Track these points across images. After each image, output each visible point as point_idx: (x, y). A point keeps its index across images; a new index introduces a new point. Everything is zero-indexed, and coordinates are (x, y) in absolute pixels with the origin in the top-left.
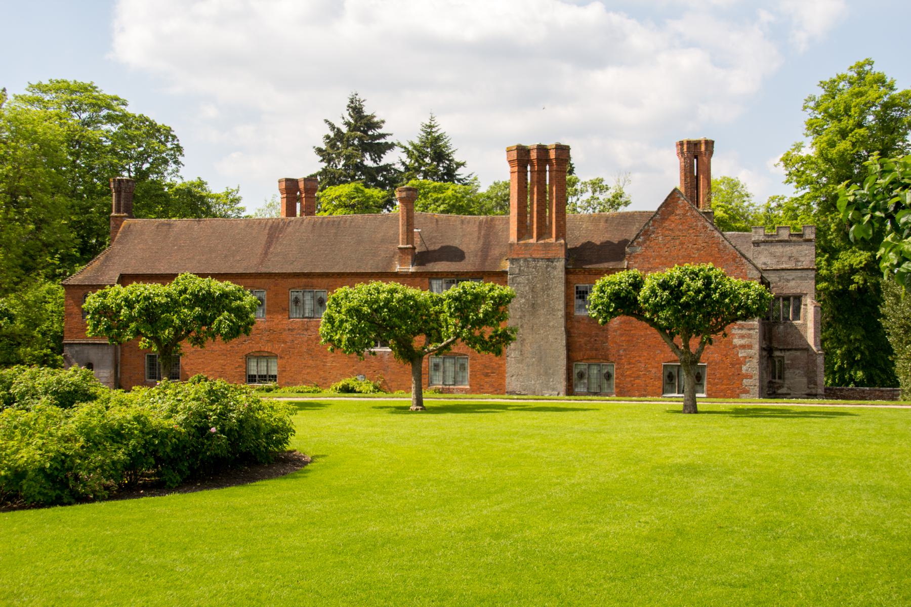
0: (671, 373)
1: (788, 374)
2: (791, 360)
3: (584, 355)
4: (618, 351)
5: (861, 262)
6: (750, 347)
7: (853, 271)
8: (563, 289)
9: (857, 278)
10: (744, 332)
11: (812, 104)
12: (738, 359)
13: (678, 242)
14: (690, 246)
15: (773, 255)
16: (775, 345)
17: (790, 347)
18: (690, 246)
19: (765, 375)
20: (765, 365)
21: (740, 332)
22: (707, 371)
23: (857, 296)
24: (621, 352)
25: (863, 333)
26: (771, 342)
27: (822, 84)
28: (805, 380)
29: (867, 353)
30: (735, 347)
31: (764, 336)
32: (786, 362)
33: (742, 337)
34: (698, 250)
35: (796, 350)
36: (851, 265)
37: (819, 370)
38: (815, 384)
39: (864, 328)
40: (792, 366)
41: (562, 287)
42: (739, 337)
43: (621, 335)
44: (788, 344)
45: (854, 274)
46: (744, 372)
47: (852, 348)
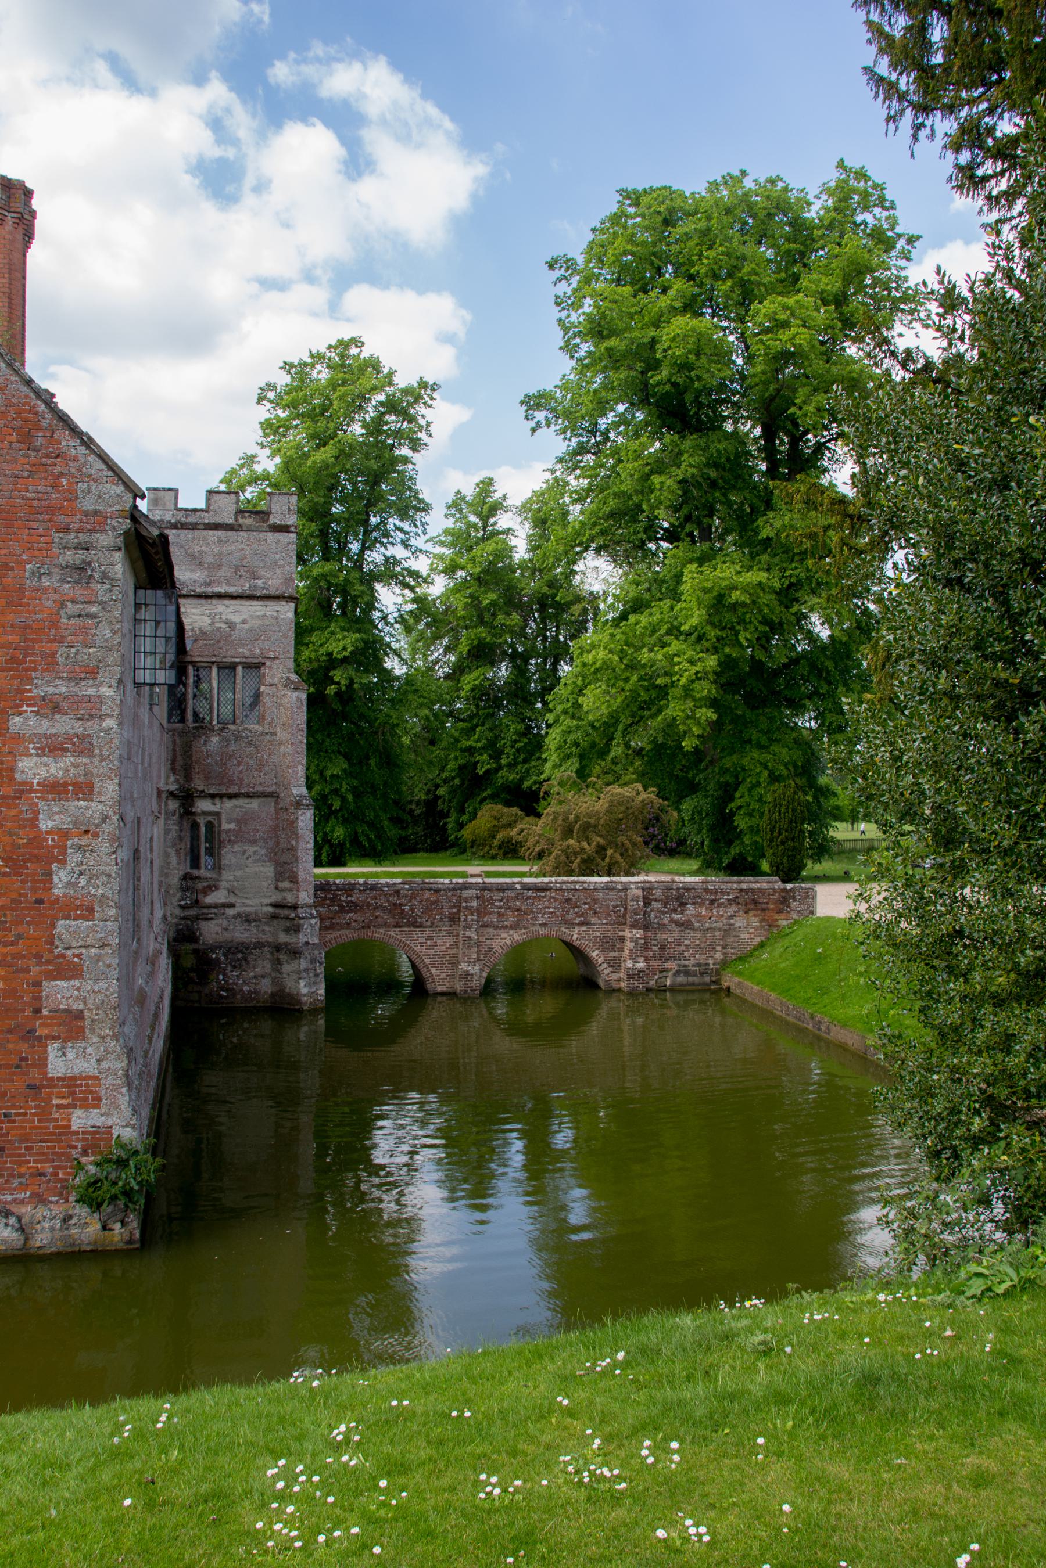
1: (229, 855)
2: (238, 822)
5: (344, 649)
6: (84, 789)
7: (332, 662)
9: (338, 675)
10: (64, 725)
11: (271, 395)
12: (37, 840)
16: (199, 784)
17: (233, 790)
19: (174, 860)
20: (173, 834)
21: (45, 726)
23: (337, 706)
25: (345, 766)
26: (188, 777)
27: (287, 366)
28: (269, 870)
29: (350, 798)
30: (24, 790)
31: (173, 762)
32: (225, 826)
33: (53, 748)
35: (248, 796)
36: (330, 654)
37: (302, 845)
38: (294, 879)
39: (346, 756)
40: (238, 836)
42: (41, 751)
44: (231, 782)
45: (334, 668)
47: (327, 790)
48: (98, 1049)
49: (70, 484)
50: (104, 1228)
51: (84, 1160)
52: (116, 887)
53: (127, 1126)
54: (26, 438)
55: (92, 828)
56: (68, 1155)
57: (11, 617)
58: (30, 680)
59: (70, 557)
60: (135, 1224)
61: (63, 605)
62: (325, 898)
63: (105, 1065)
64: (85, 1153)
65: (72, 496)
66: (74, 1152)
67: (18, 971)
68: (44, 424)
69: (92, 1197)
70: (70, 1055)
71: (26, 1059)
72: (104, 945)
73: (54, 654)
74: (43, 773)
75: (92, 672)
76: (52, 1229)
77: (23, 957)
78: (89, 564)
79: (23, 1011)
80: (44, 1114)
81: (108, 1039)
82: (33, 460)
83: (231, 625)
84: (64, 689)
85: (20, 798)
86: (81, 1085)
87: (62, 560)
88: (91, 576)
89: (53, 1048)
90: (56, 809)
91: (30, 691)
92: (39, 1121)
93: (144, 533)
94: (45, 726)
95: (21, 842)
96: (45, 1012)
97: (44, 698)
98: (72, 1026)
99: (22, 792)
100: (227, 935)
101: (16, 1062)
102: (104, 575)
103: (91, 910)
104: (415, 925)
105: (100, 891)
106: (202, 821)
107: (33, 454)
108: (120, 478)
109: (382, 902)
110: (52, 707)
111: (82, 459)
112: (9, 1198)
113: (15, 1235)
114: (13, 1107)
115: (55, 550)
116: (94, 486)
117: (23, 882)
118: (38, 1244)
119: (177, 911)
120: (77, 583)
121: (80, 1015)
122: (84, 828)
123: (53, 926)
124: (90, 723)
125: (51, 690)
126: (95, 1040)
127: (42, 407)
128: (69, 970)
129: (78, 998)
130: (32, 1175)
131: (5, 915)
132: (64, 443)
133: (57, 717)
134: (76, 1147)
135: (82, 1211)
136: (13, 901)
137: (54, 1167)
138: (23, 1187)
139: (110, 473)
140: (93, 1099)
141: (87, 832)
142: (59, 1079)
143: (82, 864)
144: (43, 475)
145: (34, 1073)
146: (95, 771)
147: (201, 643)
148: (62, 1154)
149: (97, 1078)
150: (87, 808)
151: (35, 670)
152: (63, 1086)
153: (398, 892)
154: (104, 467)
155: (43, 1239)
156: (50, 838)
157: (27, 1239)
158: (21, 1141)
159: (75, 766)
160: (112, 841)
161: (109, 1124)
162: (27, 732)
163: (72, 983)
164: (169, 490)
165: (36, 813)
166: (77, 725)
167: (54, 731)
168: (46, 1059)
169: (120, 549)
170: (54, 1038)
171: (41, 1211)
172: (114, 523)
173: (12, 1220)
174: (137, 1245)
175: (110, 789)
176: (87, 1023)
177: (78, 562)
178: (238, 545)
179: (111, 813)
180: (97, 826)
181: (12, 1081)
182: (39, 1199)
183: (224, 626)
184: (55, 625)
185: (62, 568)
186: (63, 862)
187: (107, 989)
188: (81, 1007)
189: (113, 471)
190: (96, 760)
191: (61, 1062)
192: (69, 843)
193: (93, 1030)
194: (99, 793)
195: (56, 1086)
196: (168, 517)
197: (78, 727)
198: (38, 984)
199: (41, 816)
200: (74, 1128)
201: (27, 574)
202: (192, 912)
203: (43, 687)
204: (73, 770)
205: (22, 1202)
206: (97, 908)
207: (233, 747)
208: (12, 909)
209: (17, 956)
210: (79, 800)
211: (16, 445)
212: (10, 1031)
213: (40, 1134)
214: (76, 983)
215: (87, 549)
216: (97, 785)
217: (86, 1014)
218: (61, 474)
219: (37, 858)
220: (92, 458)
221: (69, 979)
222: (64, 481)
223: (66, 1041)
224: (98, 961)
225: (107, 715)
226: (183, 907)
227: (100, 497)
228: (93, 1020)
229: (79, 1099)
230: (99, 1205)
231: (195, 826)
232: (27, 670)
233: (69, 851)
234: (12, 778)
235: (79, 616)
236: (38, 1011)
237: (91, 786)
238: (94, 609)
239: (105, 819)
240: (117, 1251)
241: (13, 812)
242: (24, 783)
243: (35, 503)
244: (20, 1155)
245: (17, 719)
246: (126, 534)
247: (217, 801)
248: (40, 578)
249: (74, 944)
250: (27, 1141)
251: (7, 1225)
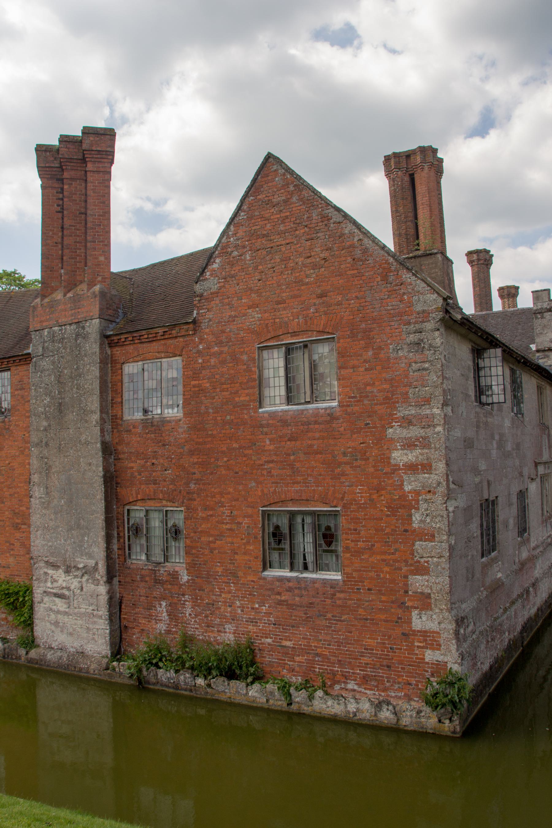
0: (277, 527)
3: (137, 494)
4: (187, 484)
6: (427, 467)
8: (98, 374)
10: (415, 432)
12: (403, 497)
13: (277, 258)
14: (300, 260)
18: (300, 260)
21: (405, 433)
22: (342, 521)
24: (192, 486)
30: (396, 469)
33: (409, 445)
34: (315, 266)
41: (95, 371)
42: (404, 447)
43: (191, 453)
46: (415, 525)
48: (439, 616)
49: (409, 298)
50: (440, 721)
51: (432, 679)
52: (447, 523)
53: (455, 663)
54: (385, 278)
55: (432, 489)
56: (423, 676)
57: (384, 375)
58: (396, 408)
59: (412, 338)
60: (457, 722)
61: (410, 365)
63: (443, 626)
64: (432, 675)
65: (410, 304)
66: (426, 674)
67: (395, 569)
68: (393, 268)
69: (433, 702)
70: (424, 618)
71: (400, 618)
72: (441, 557)
73: (408, 392)
74: (405, 459)
75: (427, 401)
76: (411, 716)
77: (398, 561)
78: (422, 340)
79: (399, 591)
80: (411, 649)
81: (444, 611)
82: (389, 289)
84: (413, 412)
85: (393, 473)
86: (430, 636)
87: (408, 341)
88: (424, 347)
89: (415, 613)
90: (412, 479)
91: (396, 414)
92: (408, 654)
93: (455, 319)
94: (405, 433)
95: (395, 497)
96: (410, 593)
97: (403, 417)
98: (425, 602)
99: (396, 470)
101: (396, 619)
102: (430, 345)
103: (433, 536)
105: (438, 526)
107: (389, 285)
108: (434, 290)
110: (408, 422)
111: (413, 283)
112: (393, 694)
113: (392, 716)
114: (395, 644)
115: (404, 336)
116: (421, 297)
117: (397, 520)
118: (404, 724)
120: (417, 352)
121: (428, 596)
122: (427, 489)
123: (413, 545)
124: (428, 430)
125: (407, 413)
126: (437, 611)
127: (391, 260)
128: (422, 570)
129: (427, 586)
130: (404, 683)
131: (389, 538)
132: (404, 276)
133: (411, 427)
134: (427, 671)
135: (427, 710)
136: (392, 530)
137: (416, 681)
138: (400, 690)
139: (429, 288)
140: (437, 645)
141: (429, 492)
142: (418, 631)
143: (428, 510)
144: (394, 296)
145: (405, 625)
146: (432, 457)
148: (421, 674)
149: (438, 633)
150: (429, 478)
151: (398, 402)
152: (420, 636)
154: (425, 285)
155: (406, 721)
156: (410, 495)
157: (398, 720)
158: (399, 664)
159: (422, 454)
160: (443, 496)
161: (446, 660)
162: (396, 437)
163: (424, 577)
164: (545, 290)
165: (402, 482)
166: (422, 431)
167: (410, 435)
168: (411, 619)
169: (438, 330)
170: (416, 608)
171: (406, 706)
172: (434, 315)
173: (391, 708)
174: (458, 735)
175: (441, 467)
176: (433, 601)
177: (416, 340)
179: (442, 480)
180: (435, 488)
181: (394, 630)
182: (409, 698)
184: (407, 377)
185: (409, 345)
186: (417, 509)
187: (443, 582)
188: (429, 591)
189: (430, 287)
190: (433, 450)
191: (419, 621)
192: (420, 498)
193: (436, 605)
194: (435, 469)
195: (416, 635)
196: (545, 305)
197: (422, 432)
198: (406, 577)
199: (405, 483)
200: (427, 660)
201: (391, 351)
203: (403, 411)
204: (420, 457)
205: (400, 698)
206: (436, 535)
208: (392, 535)
209: (395, 561)
210: (424, 473)
211: (380, 283)
212: (393, 602)
213: (409, 661)
214: (426, 577)
215: (421, 332)
216: (434, 465)
217: (432, 595)
218: (404, 294)
219: (404, 507)
220: (419, 282)
221: (422, 575)
222: (406, 297)
223: (421, 610)
224: (438, 565)
225: (437, 425)
227: (425, 302)
228: (436, 600)
229: (429, 644)
230: (436, 707)
232: (394, 403)
233: (421, 502)
234: (389, 463)
235: (419, 370)
236: (406, 592)
237: (431, 466)
238: (427, 365)
239: (439, 484)
240: (446, 736)
241: (390, 482)
242: (396, 465)
243: (392, 312)
244: (399, 672)
245: (391, 430)
246: (442, 320)
248: (397, 352)
249: (425, 555)
250: (402, 664)
251: (388, 709)
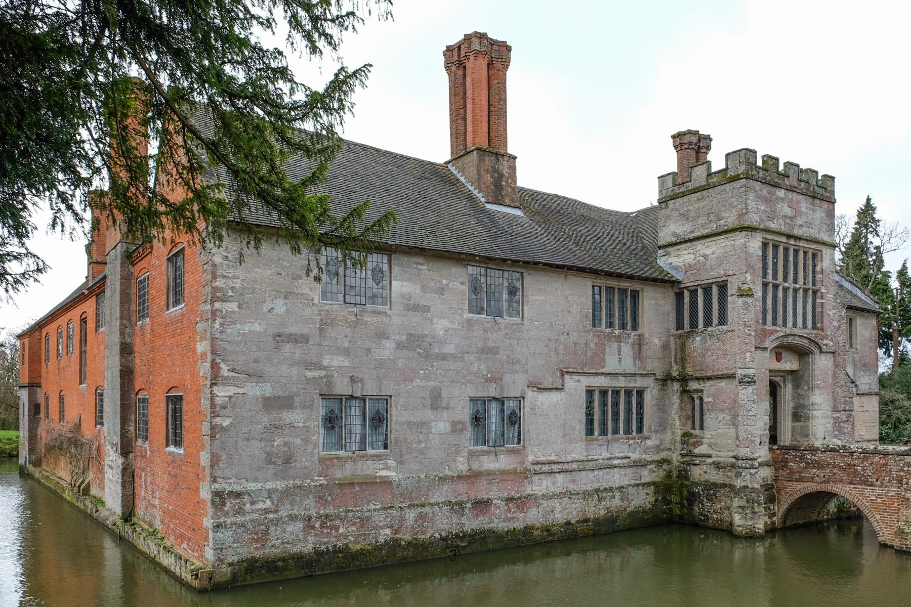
15: (685, 217)
17: (709, 374)
26: (683, 367)
62: (796, 456)
83: (705, 257)
100: (707, 477)
104: (865, 483)
106: (695, 396)
109: (839, 461)
119: (679, 457)
147: (689, 273)
153: (852, 453)
178: (710, 200)
183: (702, 258)
202: (686, 459)
207: (709, 343)
226: (682, 455)
231: (693, 399)
247: (701, 382)
